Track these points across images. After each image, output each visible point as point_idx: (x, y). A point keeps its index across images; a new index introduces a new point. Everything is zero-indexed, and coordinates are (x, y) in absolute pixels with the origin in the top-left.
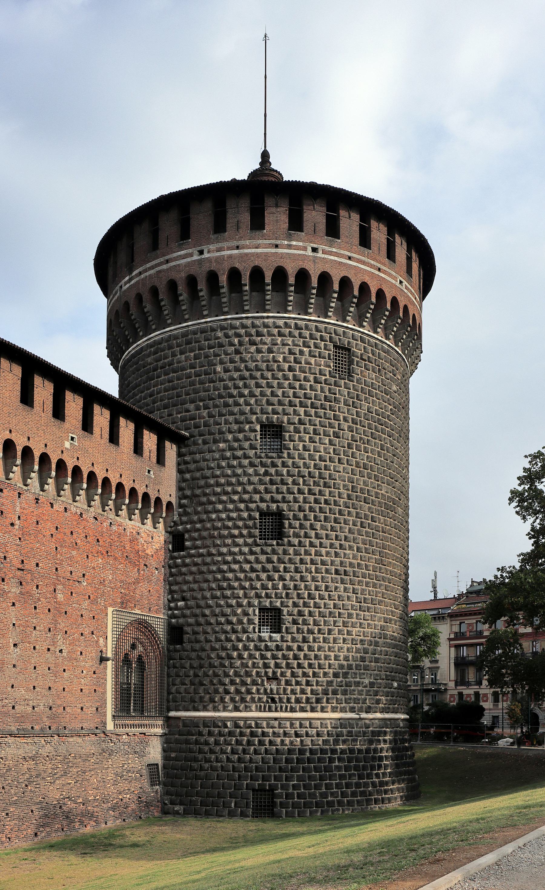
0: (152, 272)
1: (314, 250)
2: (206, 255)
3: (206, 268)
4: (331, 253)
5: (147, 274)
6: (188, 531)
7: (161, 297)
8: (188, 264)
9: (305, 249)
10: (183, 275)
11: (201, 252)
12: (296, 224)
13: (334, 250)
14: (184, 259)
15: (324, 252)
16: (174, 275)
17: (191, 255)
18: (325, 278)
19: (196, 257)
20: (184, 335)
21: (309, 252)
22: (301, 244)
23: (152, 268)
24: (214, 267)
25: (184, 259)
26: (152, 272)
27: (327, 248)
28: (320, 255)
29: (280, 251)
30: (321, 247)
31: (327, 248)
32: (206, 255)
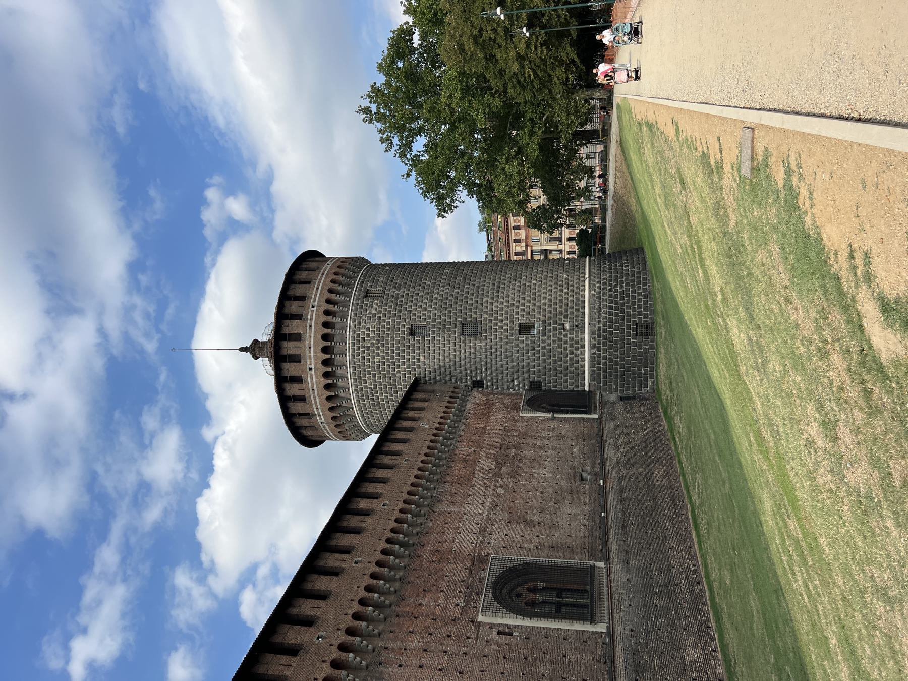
1: (313, 307)
2: (312, 366)
3: (320, 366)
4: (315, 298)
6: (471, 378)
7: (333, 394)
8: (317, 377)
10: (322, 379)
11: (311, 369)
12: (299, 317)
14: (313, 381)
16: (322, 386)
19: (313, 372)
20: (355, 380)
21: (315, 309)
23: (315, 400)
25: (313, 381)
32: (312, 366)
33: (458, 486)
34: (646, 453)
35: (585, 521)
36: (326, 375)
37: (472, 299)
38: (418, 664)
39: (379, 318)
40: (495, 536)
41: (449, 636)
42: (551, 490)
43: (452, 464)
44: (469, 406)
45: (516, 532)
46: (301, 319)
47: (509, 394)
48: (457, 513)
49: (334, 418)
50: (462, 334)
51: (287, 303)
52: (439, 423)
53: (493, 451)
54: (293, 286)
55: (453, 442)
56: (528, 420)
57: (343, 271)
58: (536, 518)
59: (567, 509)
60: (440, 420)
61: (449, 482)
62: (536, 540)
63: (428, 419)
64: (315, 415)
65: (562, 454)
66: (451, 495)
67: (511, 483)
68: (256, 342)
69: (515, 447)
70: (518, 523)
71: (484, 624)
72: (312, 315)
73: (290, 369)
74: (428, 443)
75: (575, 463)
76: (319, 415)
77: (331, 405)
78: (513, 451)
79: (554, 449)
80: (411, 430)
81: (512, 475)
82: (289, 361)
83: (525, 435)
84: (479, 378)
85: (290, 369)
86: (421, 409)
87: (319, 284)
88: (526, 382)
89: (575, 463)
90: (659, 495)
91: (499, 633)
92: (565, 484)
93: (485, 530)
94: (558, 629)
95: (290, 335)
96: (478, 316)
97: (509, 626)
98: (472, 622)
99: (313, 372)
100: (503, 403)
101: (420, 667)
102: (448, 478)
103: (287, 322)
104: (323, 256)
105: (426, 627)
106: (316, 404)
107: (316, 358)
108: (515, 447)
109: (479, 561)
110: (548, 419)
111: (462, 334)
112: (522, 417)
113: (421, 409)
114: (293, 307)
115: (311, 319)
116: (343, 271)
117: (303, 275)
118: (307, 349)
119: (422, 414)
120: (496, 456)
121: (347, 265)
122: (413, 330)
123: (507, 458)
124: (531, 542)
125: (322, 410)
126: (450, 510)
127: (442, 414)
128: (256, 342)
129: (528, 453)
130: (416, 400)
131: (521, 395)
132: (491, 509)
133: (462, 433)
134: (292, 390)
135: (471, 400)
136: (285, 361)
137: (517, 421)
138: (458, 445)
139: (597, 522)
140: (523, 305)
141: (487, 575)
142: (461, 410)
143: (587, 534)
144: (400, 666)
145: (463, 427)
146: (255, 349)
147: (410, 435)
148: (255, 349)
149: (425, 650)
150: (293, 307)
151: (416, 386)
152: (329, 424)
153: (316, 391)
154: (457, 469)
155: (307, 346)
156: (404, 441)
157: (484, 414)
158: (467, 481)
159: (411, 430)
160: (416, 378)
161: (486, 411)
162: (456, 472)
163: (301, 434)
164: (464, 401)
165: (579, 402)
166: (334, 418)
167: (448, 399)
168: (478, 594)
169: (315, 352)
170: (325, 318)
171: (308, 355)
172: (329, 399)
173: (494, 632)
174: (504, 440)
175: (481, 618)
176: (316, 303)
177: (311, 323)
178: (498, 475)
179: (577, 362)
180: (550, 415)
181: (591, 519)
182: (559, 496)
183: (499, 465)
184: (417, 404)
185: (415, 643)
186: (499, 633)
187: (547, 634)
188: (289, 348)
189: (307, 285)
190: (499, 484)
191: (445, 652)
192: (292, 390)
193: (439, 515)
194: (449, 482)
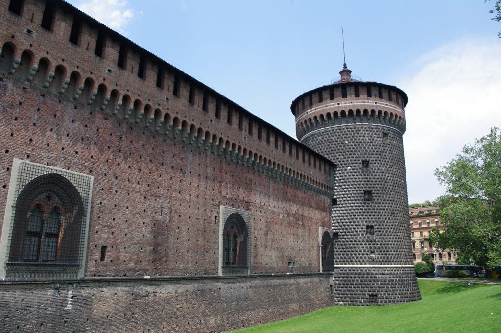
0: (321, 109)
1: (376, 103)
2: (340, 105)
3: (341, 109)
4: (381, 104)
5: (319, 110)
6: (339, 198)
7: (325, 118)
8: (334, 108)
9: (373, 103)
10: (333, 111)
11: (339, 104)
13: (382, 103)
15: (379, 104)
17: (335, 105)
18: (380, 112)
19: (337, 106)
21: (374, 104)
22: (371, 101)
23: (321, 108)
24: (343, 109)
26: (321, 109)
27: (380, 102)
28: (378, 104)
29: (365, 104)
30: (378, 102)
31: (380, 102)
33: (282, 192)
34: (304, 299)
35: (269, 264)
36: (336, 113)
37: (386, 197)
38: (201, 174)
39: (371, 142)
40: (259, 214)
41: (213, 190)
42: (283, 245)
43: (293, 188)
44: (322, 197)
45: (262, 225)
46: (368, 96)
47: (330, 221)
48: (269, 192)
49: (310, 119)
50: (365, 191)
51: (377, 89)
52: (314, 180)
53: (301, 213)
54: (387, 91)
55: (304, 188)
56: (317, 232)
57: (398, 119)
58: (269, 237)
59: (275, 254)
60: (315, 180)
61: (284, 186)
62: (259, 237)
63: (315, 173)
64: (311, 109)
65: (301, 251)
66: (278, 188)
67: (285, 223)
68: (350, 72)
69: (303, 225)
70: (267, 226)
71: (219, 209)
72: (371, 103)
73: (338, 92)
74: (303, 174)
75: (297, 259)
76: (311, 111)
77: (318, 117)
78: (301, 223)
79: (303, 247)
80: (310, 164)
81: (289, 223)
82: (342, 92)
83: (310, 230)
84: (338, 203)
85: (338, 92)
86: (320, 169)
87: (389, 106)
88: (338, 231)
89: (297, 259)
90: (284, 306)
91: (216, 217)
92: (286, 254)
93: (262, 208)
94: (218, 249)
95: (358, 91)
96: (376, 201)
97: (219, 222)
98: (220, 202)
99: (337, 106)
100: (324, 218)
101: (199, 175)
102: (286, 186)
103: (366, 89)
104: (405, 106)
105: (216, 177)
106: (318, 109)
107: (346, 107)
108: (303, 225)
109: (247, 205)
110: (318, 244)
111: (365, 191)
112: (319, 229)
113: (320, 169)
114: (375, 91)
115: (368, 102)
116: (398, 119)
117: (394, 97)
118: (351, 102)
119: (318, 170)
120: (297, 213)
121: (401, 121)
122: (366, 163)
123: (298, 220)
124: (258, 234)
125: (315, 112)
126: (271, 187)
127: (318, 181)
128: (350, 72)
129: (300, 231)
130: (325, 166)
131: (330, 228)
132: (272, 211)
133: (308, 194)
134: (326, 95)
135: (326, 198)
136: (342, 89)
137: (317, 226)
138: (303, 191)
139: (269, 271)
140: (385, 228)
141: (242, 211)
142: (320, 192)
143: (263, 265)
144: (199, 164)
145: (312, 194)
146: (346, 72)
147: (307, 164)
148: (346, 72)
149: (206, 177)
150: (375, 91)
151: (332, 166)
152: (307, 116)
153: (326, 108)
154: (290, 191)
155: (352, 101)
156: (304, 160)
157: (319, 206)
158: (286, 198)
159: (310, 164)
160: (336, 165)
161: (320, 208)
162: (289, 191)
163: (300, 101)
164: (325, 194)
165: (328, 263)
166: (310, 119)
167: (326, 184)
168: (232, 205)
169: (349, 106)
170: (369, 110)
171: (347, 102)
172: (322, 116)
173: (216, 214)
174: (307, 218)
175: (222, 207)
176: (378, 104)
177: (366, 102)
178: (289, 215)
179: (352, 261)
180: (320, 244)
181: (271, 268)
182: (280, 249)
183: (294, 215)
184: (323, 166)
185: (210, 172)
186: (216, 217)
187: (216, 243)
188: (351, 91)
189: (388, 99)
190: (284, 215)
191: (206, 188)
192: (326, 95)
193: (268, 182)
194: (284, 186)
